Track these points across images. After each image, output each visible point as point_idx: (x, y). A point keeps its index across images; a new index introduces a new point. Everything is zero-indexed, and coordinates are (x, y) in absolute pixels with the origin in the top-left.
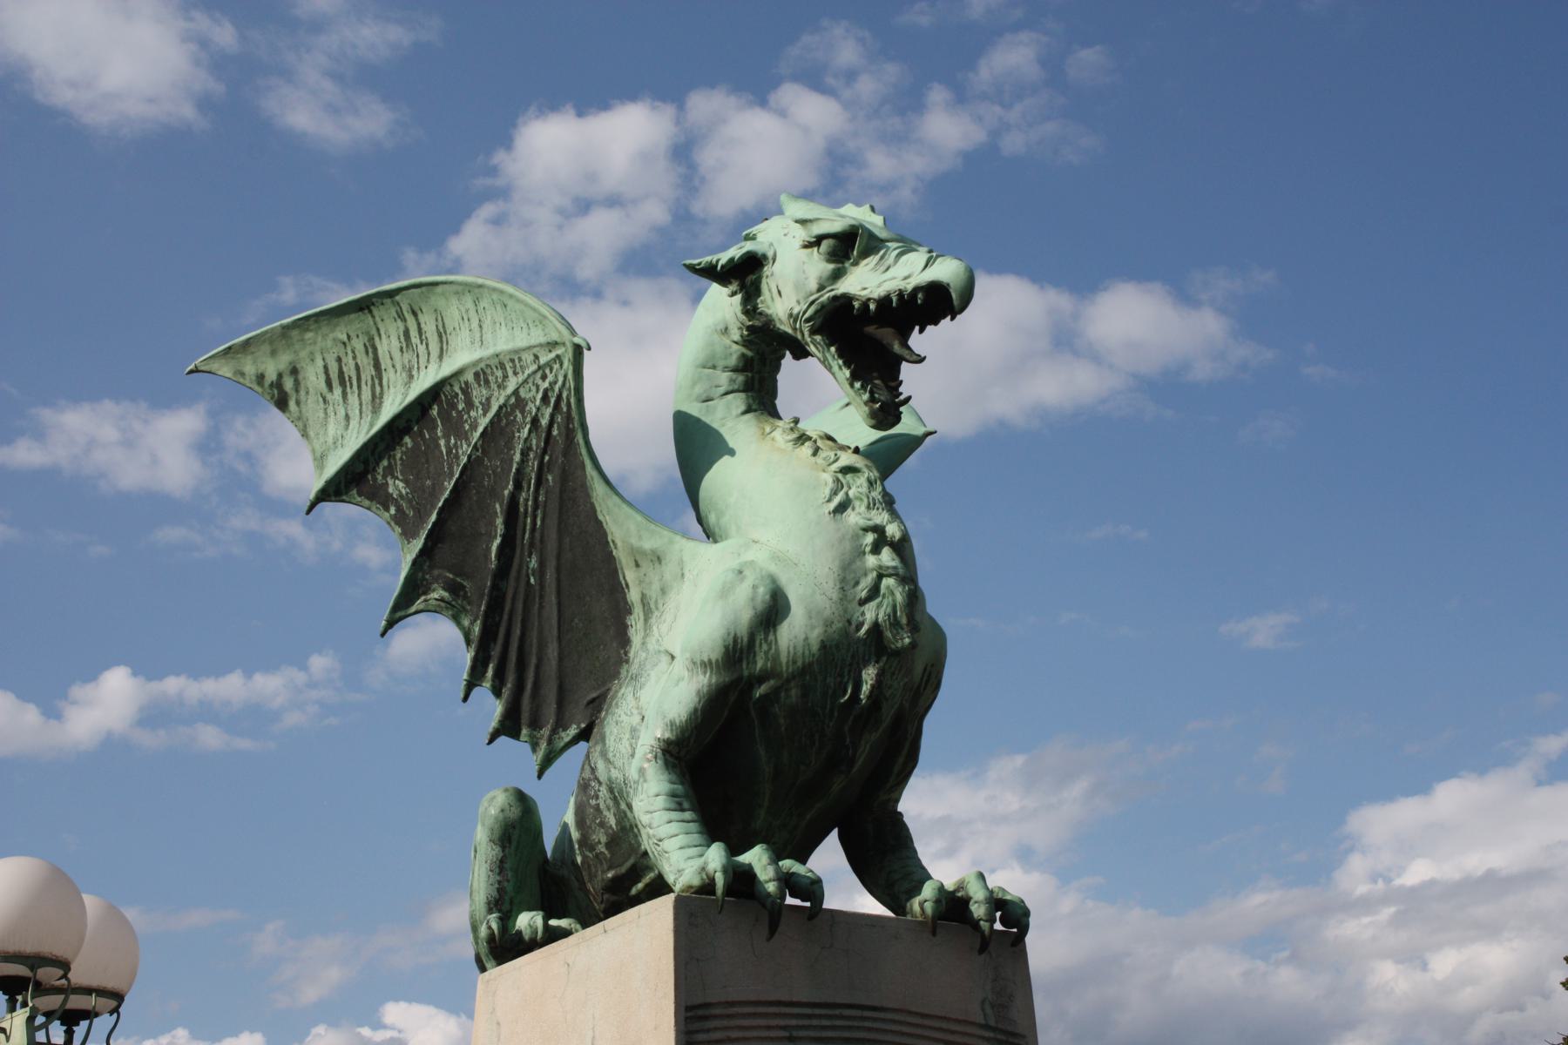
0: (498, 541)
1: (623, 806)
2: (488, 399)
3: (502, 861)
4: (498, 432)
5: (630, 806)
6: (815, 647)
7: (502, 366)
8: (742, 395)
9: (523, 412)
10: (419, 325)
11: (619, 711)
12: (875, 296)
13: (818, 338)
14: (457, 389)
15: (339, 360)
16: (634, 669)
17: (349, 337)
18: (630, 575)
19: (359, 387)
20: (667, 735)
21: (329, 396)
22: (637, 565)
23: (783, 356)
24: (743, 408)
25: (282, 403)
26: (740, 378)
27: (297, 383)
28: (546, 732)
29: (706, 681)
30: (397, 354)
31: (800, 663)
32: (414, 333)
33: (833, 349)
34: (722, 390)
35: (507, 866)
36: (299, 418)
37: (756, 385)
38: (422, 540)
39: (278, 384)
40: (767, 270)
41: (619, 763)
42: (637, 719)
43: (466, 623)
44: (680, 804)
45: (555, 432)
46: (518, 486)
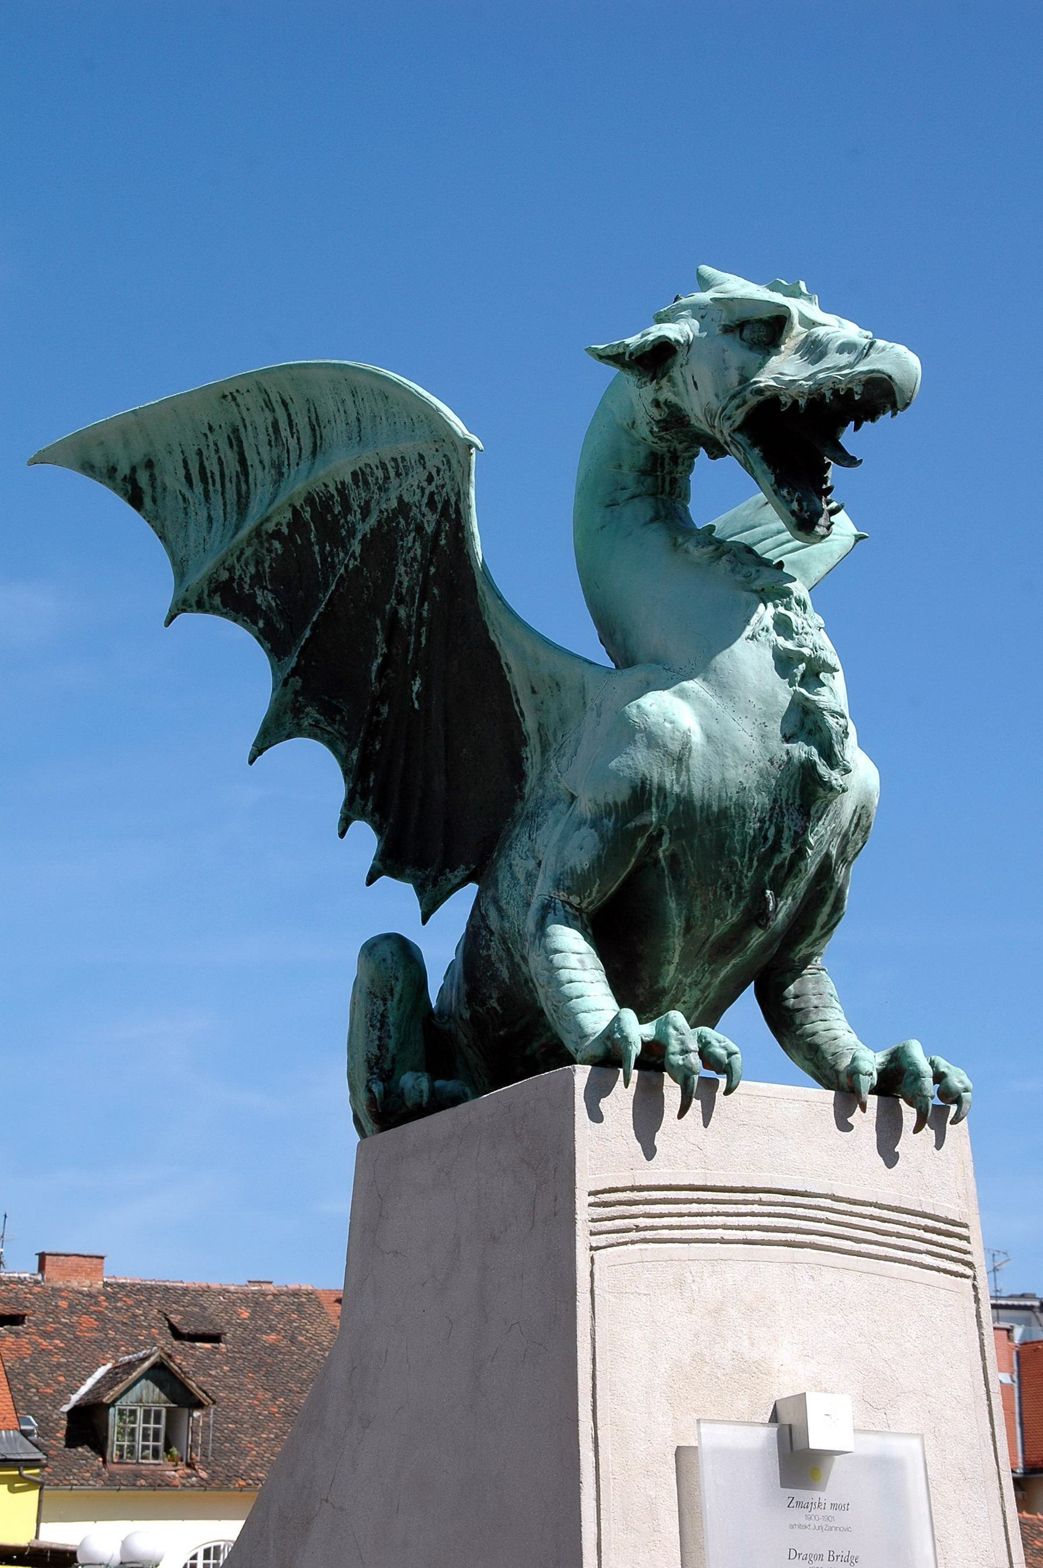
0: (380, 660)
1: (517, 958)
2: (368, 503)
3: (382, 1015)
4: (383, 543)
5: (524, 959)
6: (733, 791)
8: (651, 500)
10: (289, 415)
11: (513, 853)
13: (739, 437)
14: (332, 489)
15: (200, 453)
16: (530, 806)
17: (211, 428)
18: (526, 703)
19: (223, 485)
20: (568, 883)
21: (188, 495)
22: (534, 692)
23: (696, 455)
24: (650, 514)
25: (136, 500)
26: (649, 480)
27: (152, 478)
28: (431, 871)
29: (611, 825)
30: (265, 450)
31: (715, 809)
32: (283, 424)
33: (757, 450)
34: (627, 494)
35: (391, 1020)
36: (156, 518)
37: (667, 488)
38: (295, 659)
39: (131, 479)
40: (680, 359)
41: (511, 911)
42: (531, 864)
43: (344, 751)
44: (581, 962)
45: (443, 542)
46: (401, 601)
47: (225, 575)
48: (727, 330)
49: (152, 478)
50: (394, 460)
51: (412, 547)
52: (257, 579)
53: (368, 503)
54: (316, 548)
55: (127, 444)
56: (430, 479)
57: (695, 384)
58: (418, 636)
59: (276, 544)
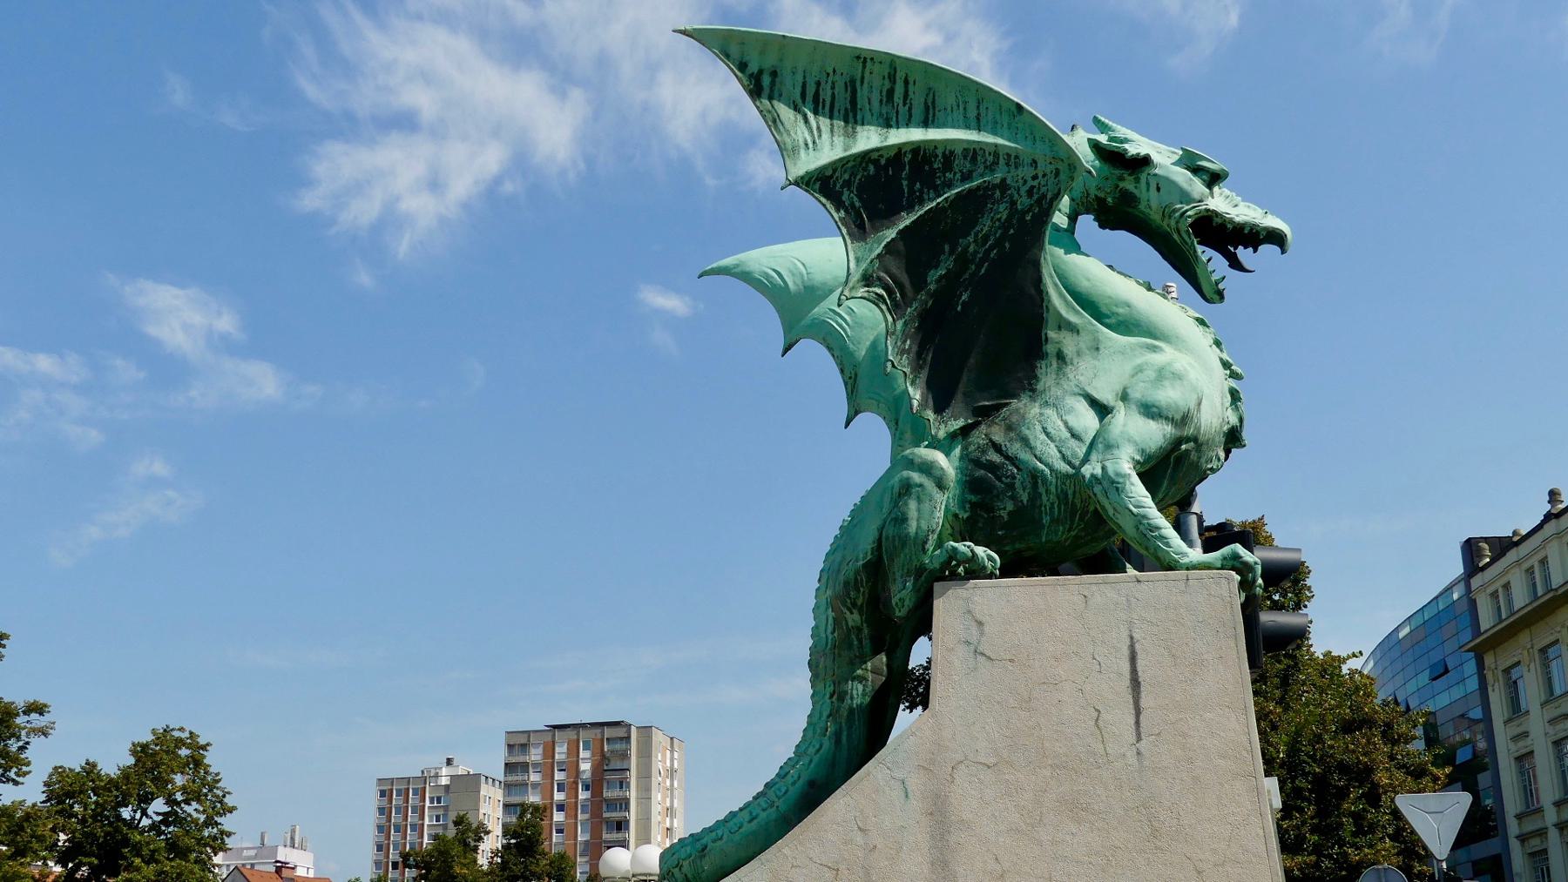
1: (1042, 490)
2: (971, 172)
4: (974, 203)
7: (996, 155)
9: (1003, 193)
12: (1237, 219)
14: (939, 152)
20: (1138, 457)
25: (755, 92)
30: (876, 104)
47: (829, 173)
48: (1188, 168)
49: (773, 84)
50: (1009, 155)
51: (1003, 211)
52: (848, 184)
53: (971, 172)
54: (905, 183)
55: (762, 53)
56: (1035, 177)
57: (1158, 189)
58: (979, 267)
59: (871, 168)
